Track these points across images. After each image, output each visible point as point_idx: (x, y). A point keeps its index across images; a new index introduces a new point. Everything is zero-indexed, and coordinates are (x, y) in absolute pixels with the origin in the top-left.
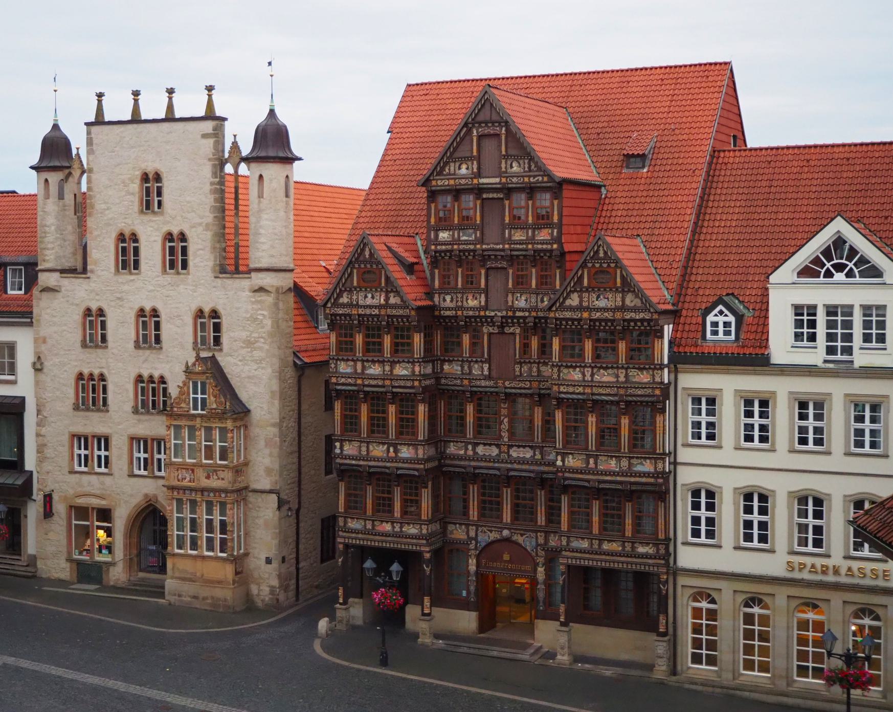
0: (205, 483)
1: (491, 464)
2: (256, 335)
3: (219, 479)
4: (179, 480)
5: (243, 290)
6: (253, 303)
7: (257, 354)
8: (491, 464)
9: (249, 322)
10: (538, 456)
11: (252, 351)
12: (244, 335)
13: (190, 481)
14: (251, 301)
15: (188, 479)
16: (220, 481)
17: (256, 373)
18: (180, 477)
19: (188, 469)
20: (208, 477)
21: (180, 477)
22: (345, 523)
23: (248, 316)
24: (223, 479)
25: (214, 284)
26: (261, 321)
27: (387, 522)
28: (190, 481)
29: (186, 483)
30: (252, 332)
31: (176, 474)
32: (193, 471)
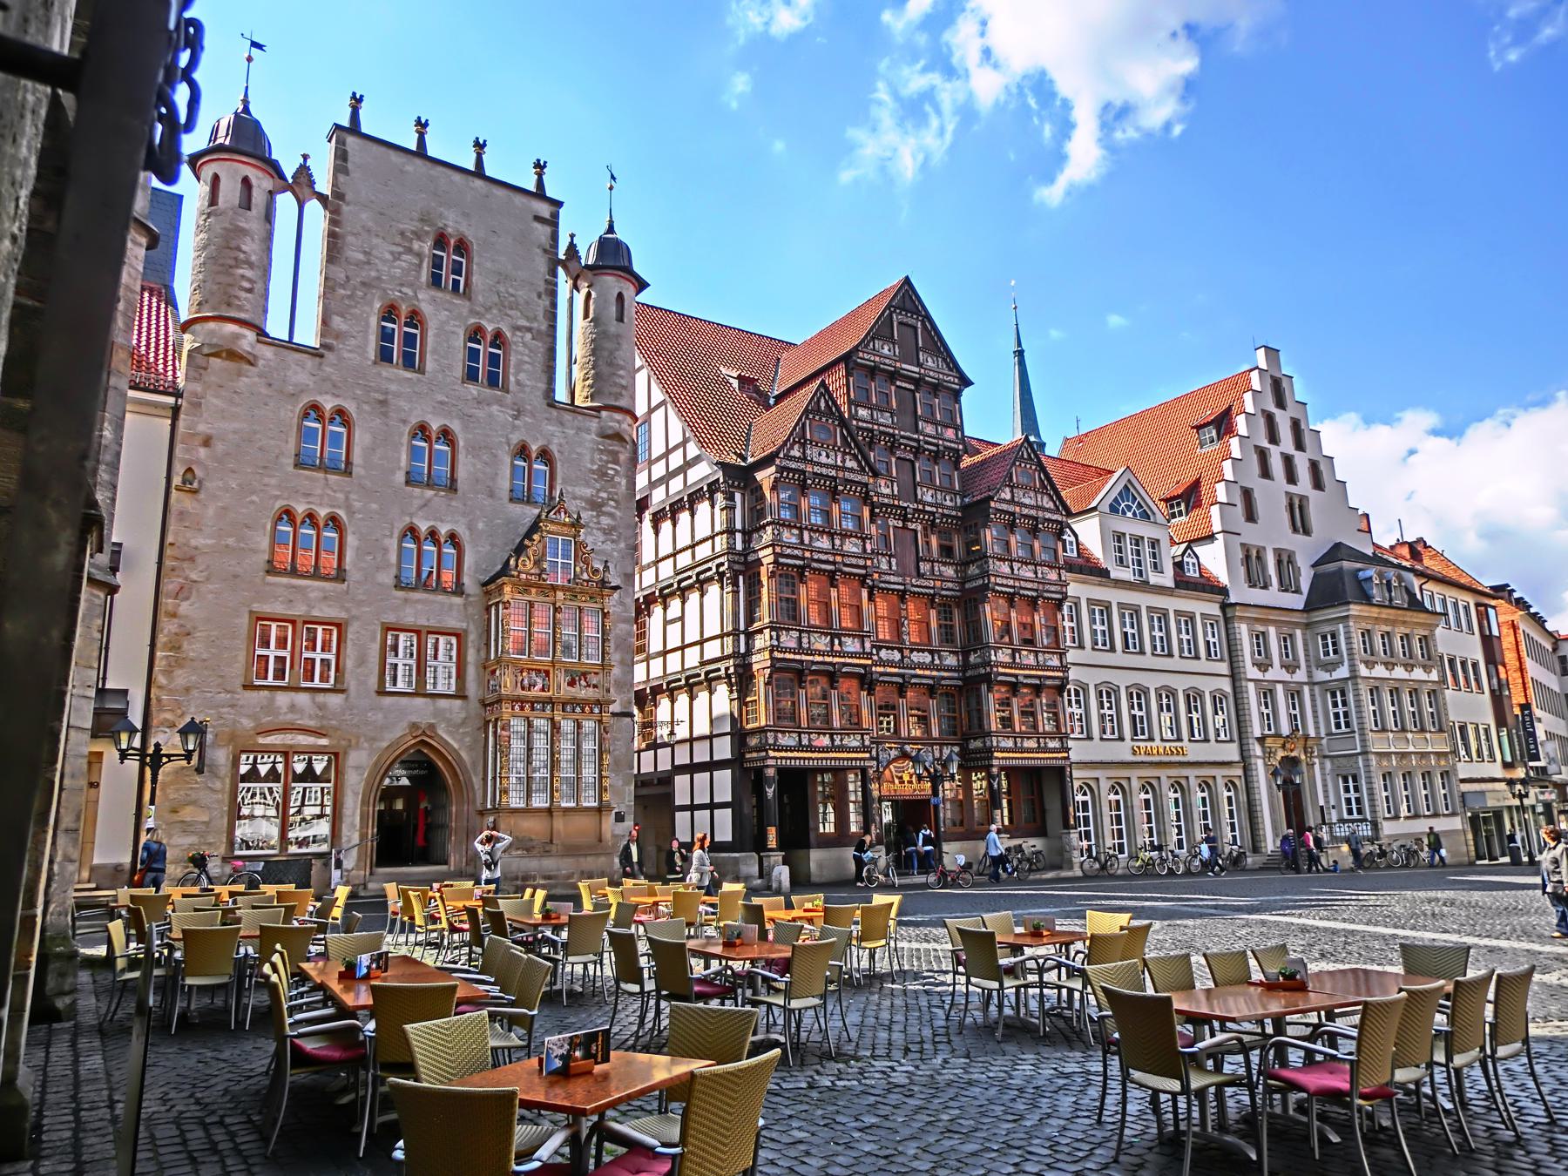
1: (896, 670)
2: (604, 495)
4: (523, 688)
5: (588, 431)
6: (601, 452)
7: (606, 521)
8: (896, 670)
10: (937, 662)
11: (598, 516)
12: (588, 492)
13: (543, 690)
15: (539, 686)
16: (591, 689)
17: (604, 546)
18: (526, 682)
19: (539, 671)
21: (526, 682)
22: (776, 739)
23: (595, 467)
24: (595, 686)
25: (547, 415)
26: (612, 478)
27: (824, 734)
28: (543, 690)
29: (535, 692)
30: (599, 491)
32: (547, 673)
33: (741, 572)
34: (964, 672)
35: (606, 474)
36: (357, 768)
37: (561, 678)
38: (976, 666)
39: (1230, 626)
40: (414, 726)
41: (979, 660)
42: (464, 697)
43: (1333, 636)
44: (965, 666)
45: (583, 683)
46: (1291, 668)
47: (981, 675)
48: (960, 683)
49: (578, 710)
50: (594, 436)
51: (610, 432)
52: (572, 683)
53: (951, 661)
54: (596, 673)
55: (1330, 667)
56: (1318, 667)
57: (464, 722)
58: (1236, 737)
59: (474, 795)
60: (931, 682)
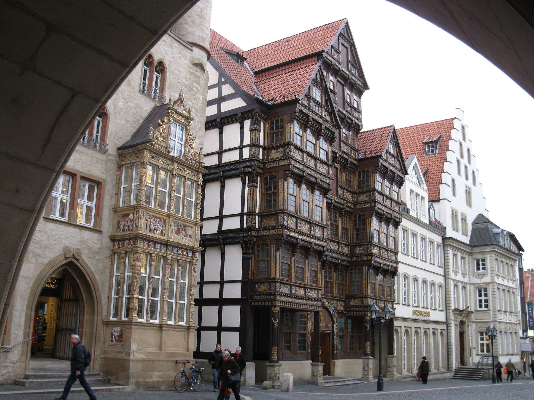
0: (175, 238)
3: (187, 236)
4: (150, 231)
9: (187, 89)
13: (162, 234)
14: (190, 71)
16: (188, 238)
19: (160, 219)
20: (178, 232)
21: (152, 226)
23: (187, 83)
24: (190, 237)
26: (196, 93)
28: (162, 234)
29: (157, 235)
31: (149, 223)
32: (165, 221)
33: (259, 174)
34: (351, 258)
35: (192, 89)
36: (26, 278)
37: (172, 227)
38: (360, 255)
39: (446, 249)
40: (66, 250)
41: (363, 252)
42: (100, 232)
43: (483, 260)
44: (352, 255)
45: (184, 234)
46: (464, 275)
47: (363, 261)
48: (348, 264)
49: (180, 253)
50: (188, 62)
51: (197, 62)
52: (178, 232)
53: (346, 250)
54: (191, 227)
55: (480, 276)
56: (473, 275)
57: (98, 253)
58: (444, 309)
59: (102, 308)
60: (336, 261)
